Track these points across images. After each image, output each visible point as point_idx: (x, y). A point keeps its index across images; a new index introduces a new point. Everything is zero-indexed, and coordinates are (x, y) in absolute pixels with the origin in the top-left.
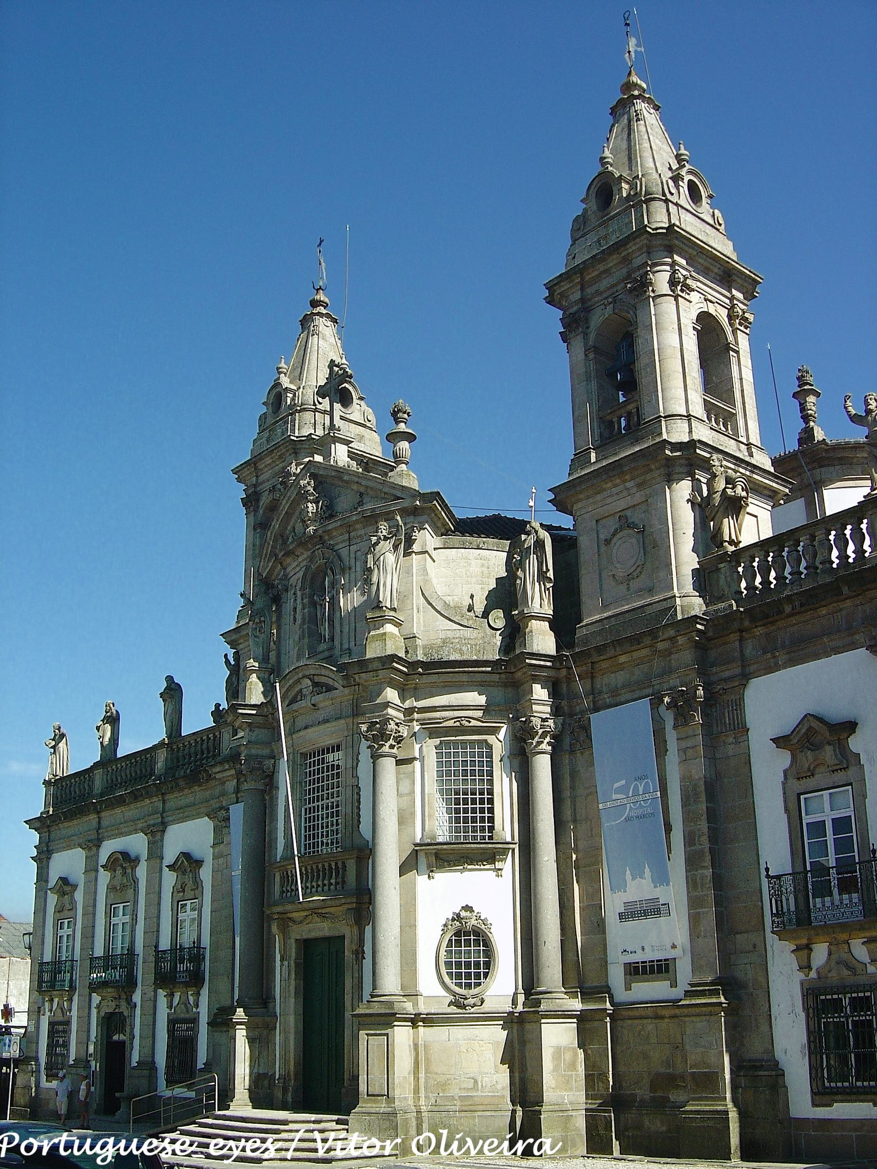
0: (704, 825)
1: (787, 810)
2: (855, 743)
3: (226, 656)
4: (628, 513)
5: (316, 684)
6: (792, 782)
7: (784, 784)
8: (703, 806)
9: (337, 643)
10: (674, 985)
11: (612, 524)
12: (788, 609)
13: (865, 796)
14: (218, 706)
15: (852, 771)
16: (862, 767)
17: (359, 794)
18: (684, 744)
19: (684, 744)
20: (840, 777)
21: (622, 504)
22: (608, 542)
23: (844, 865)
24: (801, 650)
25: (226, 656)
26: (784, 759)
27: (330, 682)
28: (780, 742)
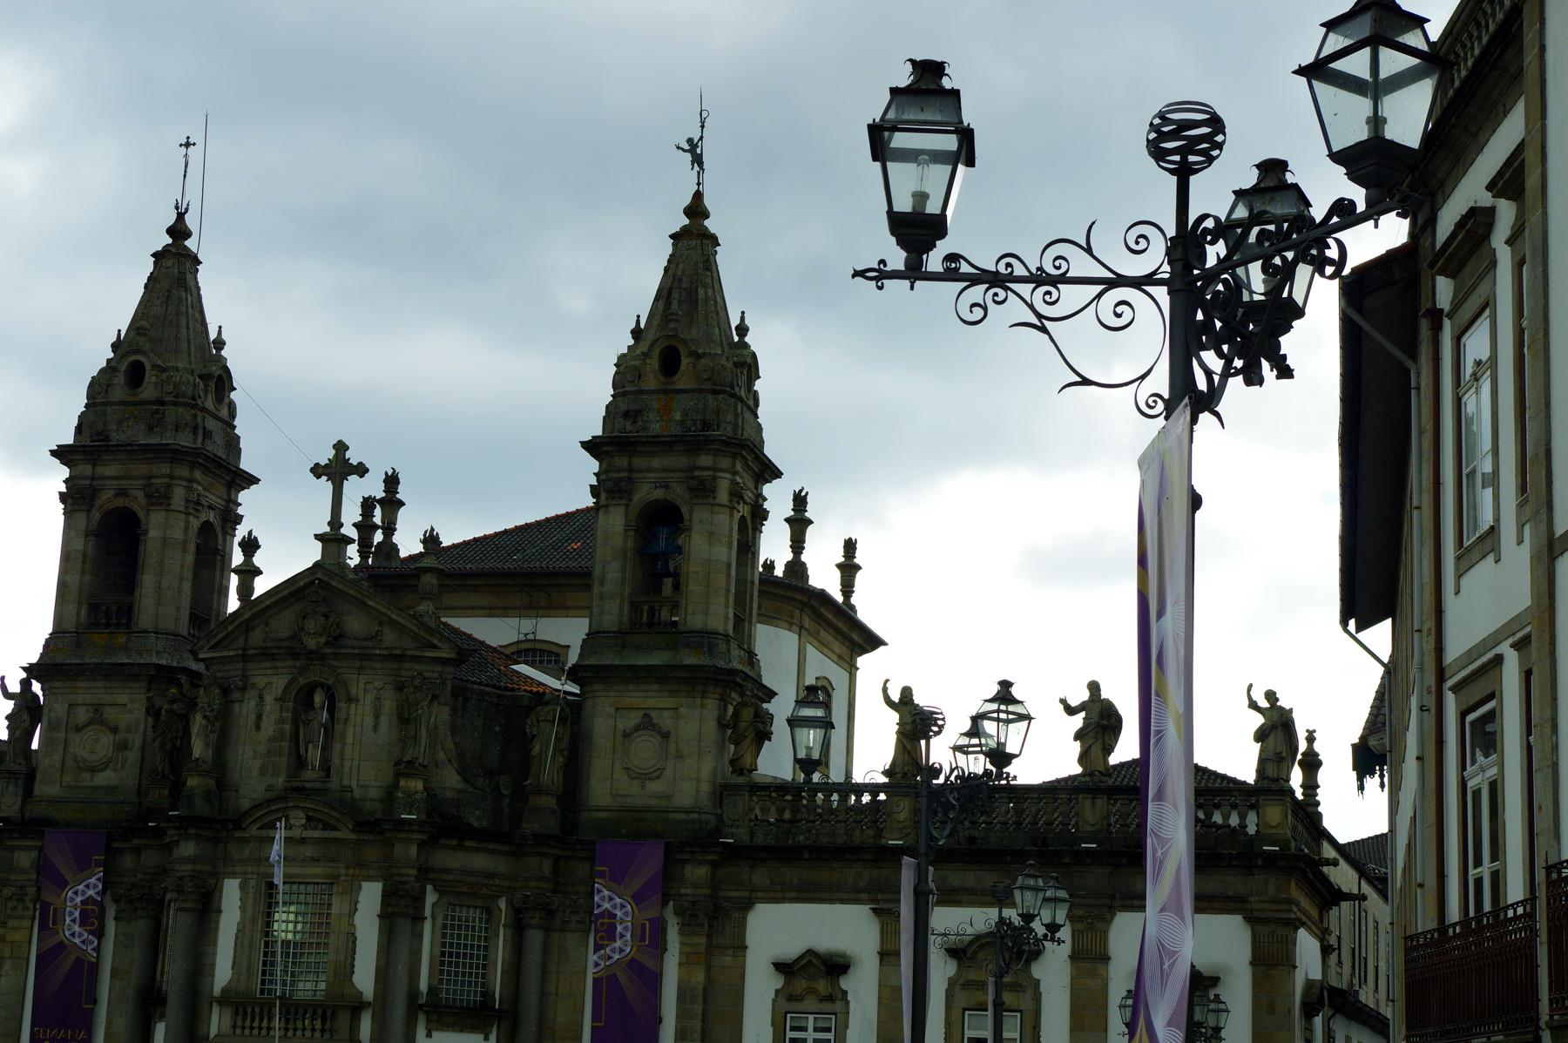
0: (697, 1025)
1: (773, 1024)
2: (844, 983)
4: (653, 714)
5: (309, 818)
7: (774, 1001)
8: (698, 1008)
9: (334, 778)
11: (635, 718)
12: (806, 855)
13: (847, 1027)
15: (839, 1006)
16: (847, 1003)
17: (354, 942)
19: (687, 950)
20: (827, 1007)
21: (650, 703)
22: (626, 735)
26: (778, 982)
28: (780, 967)
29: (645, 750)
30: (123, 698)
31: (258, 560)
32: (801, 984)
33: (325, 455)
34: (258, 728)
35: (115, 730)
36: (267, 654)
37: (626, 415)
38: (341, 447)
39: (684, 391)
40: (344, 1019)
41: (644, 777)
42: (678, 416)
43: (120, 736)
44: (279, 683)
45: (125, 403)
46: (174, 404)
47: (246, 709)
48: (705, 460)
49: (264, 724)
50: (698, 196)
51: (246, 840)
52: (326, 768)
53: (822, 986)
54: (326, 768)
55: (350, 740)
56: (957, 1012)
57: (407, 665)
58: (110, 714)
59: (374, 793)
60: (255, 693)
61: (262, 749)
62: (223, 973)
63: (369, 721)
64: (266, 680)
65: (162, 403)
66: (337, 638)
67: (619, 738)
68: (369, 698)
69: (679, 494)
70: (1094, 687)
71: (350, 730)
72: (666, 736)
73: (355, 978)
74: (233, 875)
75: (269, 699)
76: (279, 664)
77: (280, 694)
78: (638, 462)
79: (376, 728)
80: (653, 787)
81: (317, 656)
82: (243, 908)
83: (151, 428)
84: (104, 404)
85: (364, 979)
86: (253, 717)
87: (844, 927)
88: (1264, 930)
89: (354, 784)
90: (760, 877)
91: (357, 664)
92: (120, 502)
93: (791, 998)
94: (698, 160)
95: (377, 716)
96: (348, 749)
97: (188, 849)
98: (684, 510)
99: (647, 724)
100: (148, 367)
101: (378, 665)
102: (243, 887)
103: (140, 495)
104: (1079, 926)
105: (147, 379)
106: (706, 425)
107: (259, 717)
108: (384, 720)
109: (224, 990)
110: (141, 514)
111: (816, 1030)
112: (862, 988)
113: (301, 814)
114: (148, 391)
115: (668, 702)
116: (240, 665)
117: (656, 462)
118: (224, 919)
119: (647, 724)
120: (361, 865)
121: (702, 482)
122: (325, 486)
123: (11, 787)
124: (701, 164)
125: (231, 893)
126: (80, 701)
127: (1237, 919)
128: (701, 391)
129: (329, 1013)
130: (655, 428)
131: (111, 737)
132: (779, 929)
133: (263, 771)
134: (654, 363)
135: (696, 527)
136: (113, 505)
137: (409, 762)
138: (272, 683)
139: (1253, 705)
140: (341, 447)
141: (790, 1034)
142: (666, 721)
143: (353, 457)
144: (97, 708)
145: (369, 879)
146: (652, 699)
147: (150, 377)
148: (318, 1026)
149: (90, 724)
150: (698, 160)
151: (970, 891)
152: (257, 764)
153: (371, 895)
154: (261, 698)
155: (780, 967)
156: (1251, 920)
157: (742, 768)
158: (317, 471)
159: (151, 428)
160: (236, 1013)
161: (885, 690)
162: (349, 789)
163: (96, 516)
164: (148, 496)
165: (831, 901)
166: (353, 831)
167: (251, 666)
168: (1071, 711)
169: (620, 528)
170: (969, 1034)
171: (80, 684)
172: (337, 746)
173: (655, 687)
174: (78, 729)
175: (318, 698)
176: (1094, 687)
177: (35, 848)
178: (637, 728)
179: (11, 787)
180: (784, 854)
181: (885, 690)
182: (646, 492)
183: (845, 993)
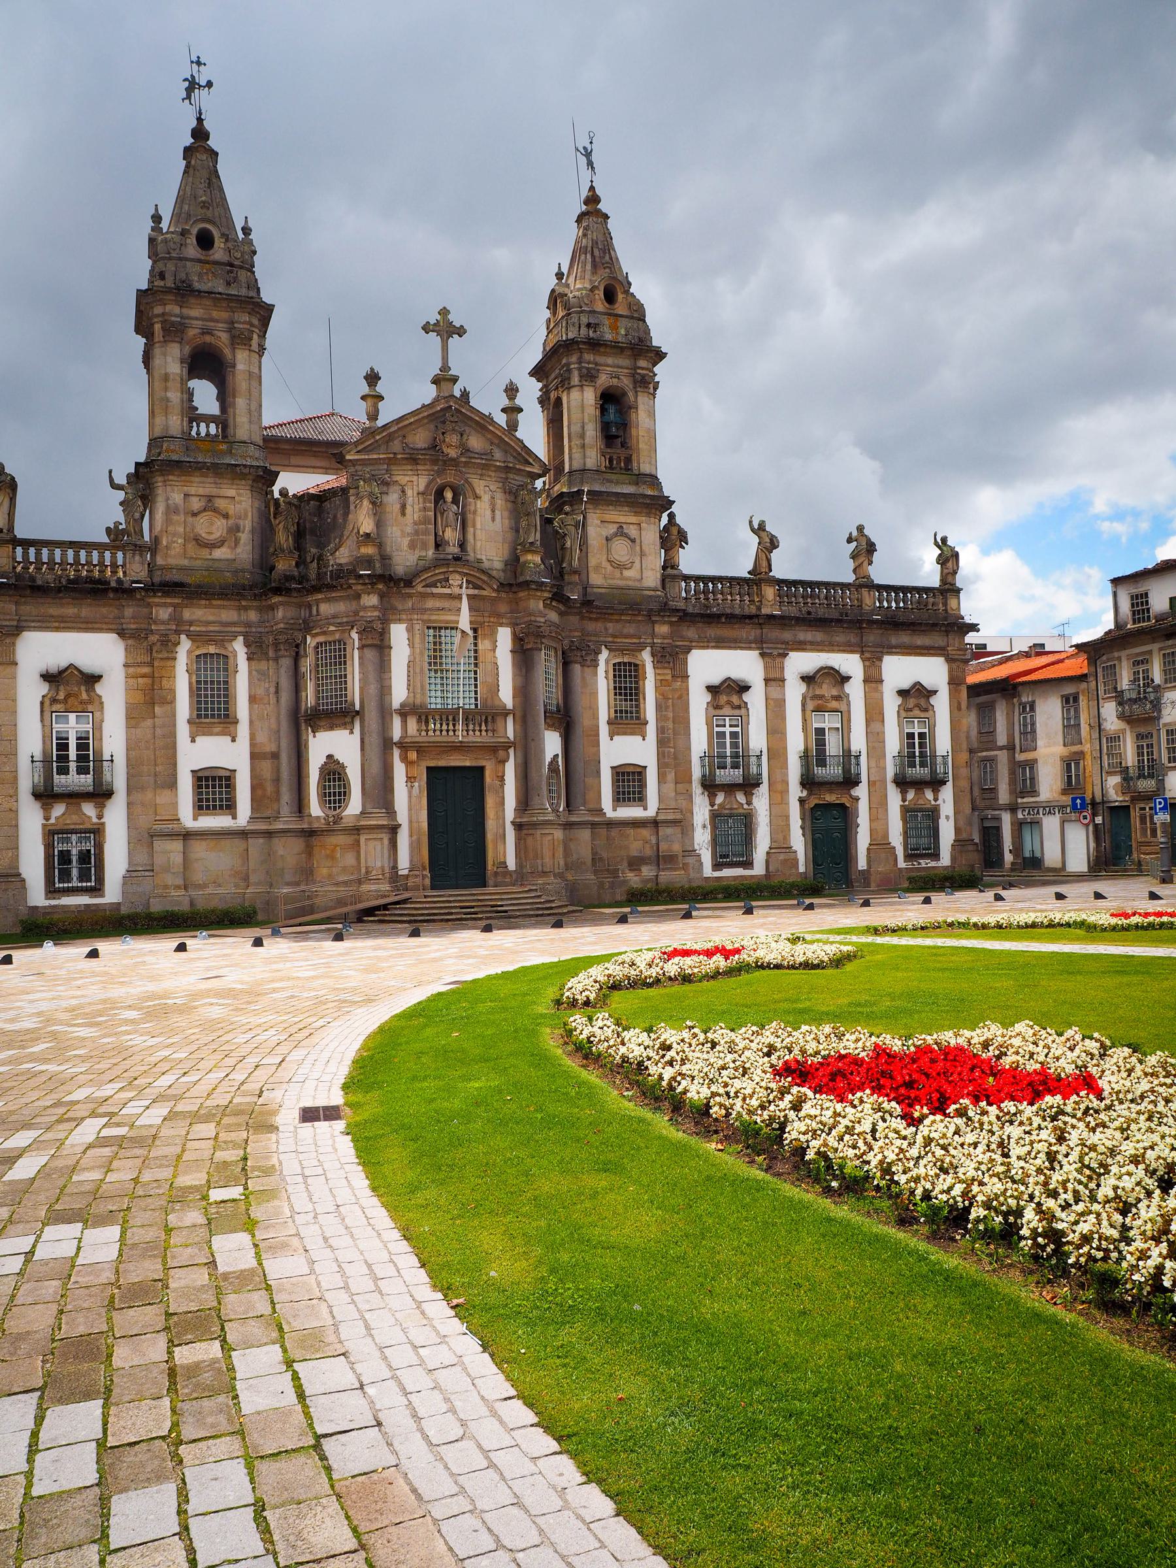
3: (110, 472)
6: (711, 709)
10: (646, 809)
11: (613, 529)
14: (117, 524)
15: (743, 711)
18: (659, 677)
19: (659, 677)
20: (737, 712)
21: (622, 519)
23: (735, 755)
24: (721, 643)
25: (110, 472)
27: (480, 583)
28: (711, 689)
29: (620, 550)
30: (231, 493)
31: (380, 388)
32: (723, 699)
33: (433, 317)
34: (403, 514)
35: (226, 516)
36: (412, 459)
37: (589, 325)
38: (444, 312)
39: (621, 316)
40: (499, 720)
41: (621, 567)
42: (623, 332)
43: (231, 522)
44: (422, 482)
45: (199, 261)
46: (241, 267)
47: (392, 499)
48: (642, 363)
49: (409, 509)
50: (592, 188)
51: (410, 596)
52: (462, 545)
53: (735, 699)
54: (462, 545)
55: (478, 526)
56: (808, 713)
57: (511, 476)
58: (221, 504)
59: (498, 565)
60: (398, 488)
61: (409, 529)
62: (399, 693)
63: (488, 513)
64: (407, 478)
65: (231, 265)
66: (466, 450)
67: (604, 541)
68: (486, 498)
69: (626, 383)
70: (860, 529)
71: (478, 519)
72: (633, 541)
73: (500, 694)
74: (400, 621)
75: (409, 493)
76: (419, 467)
77: (422, 488)
78: (601, 359)
79: (493, 519)
80: (627, 573)
81: (454, 462)
82: (411, 645)
83: (228, 284)
84: (180, 259)
85: (506, 695)
86: (397, 507)
87: (744, 664)
88: (954, 666)
89: (484, 558)
90: (691, 633)
91: (480, 472)
92: (208, 339)
93: (717, 707)
94: (590, 164)
95: (493, 511)
96: (478, 532)
97: (371, 600)
98: (631, 395)
99: (621, 532)
100: (216, 233)
101: (493, 474)
102: (410, 630)
103: (224, 337)
104: (867, 663)
105: (216, 245)
106: (640, 340)
107: (403, 507)
108: (498, 513)
109: (403, 705)
110: (227, 352)
111: (731, 726)
112: (756, 700)
113: (458, 577)
114: (219, 252)
115: (634, 519)
116: (385, 467)
117: (610, 361)
118: (393, 652)
119: (621, 532)
120: (499, 616)
121: (643, 376)
122: (434, 339)
123: (137, 558)
124: (593, 168)
125: (398, 634)
126: (192, 491)
127: (941, 660)
128: (632, 318)
129: (490, 718)
130: (609, 336)
131: (224, 521)
132: (708, 665)
133: (412, 546)
134: (600, 294)
135: (641, 407)
136: (199, 341)
137: (531, 543)
138: (414, 483)
139: (936, 544)
140: (444, 312)
141: (717, 729)
142: (633, 531)
143: (456, 319)
144: (210, 498)
145: (501, 625)
146: (626, 517)
147: (219, 243)
148: (483, 727)
149: (205, 510)
150: (590, 164)
151: (811, 643)
152: (405, 542)
153: (504, 636)
154: (403, 491)
155: (711, 689)
156: (949, 660)
157: (669, 565)
158: (426, 328)
159: (228, 284)
160: (419, 721)
161: (751, 522)
162: (479, 561)
163: (187, 349)
164: (233, 338)
165: (735, 648)
166: (497, 591)
167: (393, 468)
168: (850, 540)
169: (593, 402)
170: (815, 725)
171: (192, 479)
172: (470, 530)
173: (626, 509)
174: (195, 515)
175: (449, 495)
176: (860, 529)
177: (171, 605)
178: (616, 535)
179: (137, 558)
180: (710, 618)
181: (751, 522)
182: (603, 380)
183: (746, 703)
